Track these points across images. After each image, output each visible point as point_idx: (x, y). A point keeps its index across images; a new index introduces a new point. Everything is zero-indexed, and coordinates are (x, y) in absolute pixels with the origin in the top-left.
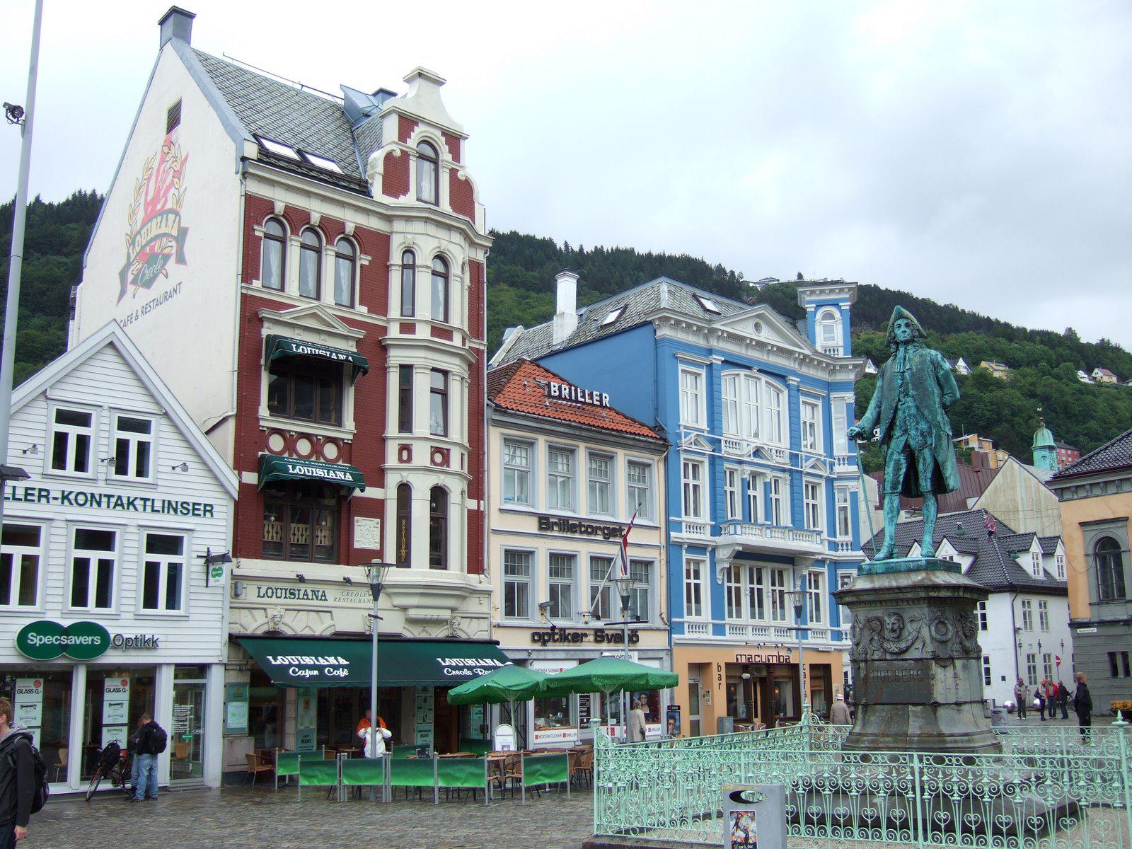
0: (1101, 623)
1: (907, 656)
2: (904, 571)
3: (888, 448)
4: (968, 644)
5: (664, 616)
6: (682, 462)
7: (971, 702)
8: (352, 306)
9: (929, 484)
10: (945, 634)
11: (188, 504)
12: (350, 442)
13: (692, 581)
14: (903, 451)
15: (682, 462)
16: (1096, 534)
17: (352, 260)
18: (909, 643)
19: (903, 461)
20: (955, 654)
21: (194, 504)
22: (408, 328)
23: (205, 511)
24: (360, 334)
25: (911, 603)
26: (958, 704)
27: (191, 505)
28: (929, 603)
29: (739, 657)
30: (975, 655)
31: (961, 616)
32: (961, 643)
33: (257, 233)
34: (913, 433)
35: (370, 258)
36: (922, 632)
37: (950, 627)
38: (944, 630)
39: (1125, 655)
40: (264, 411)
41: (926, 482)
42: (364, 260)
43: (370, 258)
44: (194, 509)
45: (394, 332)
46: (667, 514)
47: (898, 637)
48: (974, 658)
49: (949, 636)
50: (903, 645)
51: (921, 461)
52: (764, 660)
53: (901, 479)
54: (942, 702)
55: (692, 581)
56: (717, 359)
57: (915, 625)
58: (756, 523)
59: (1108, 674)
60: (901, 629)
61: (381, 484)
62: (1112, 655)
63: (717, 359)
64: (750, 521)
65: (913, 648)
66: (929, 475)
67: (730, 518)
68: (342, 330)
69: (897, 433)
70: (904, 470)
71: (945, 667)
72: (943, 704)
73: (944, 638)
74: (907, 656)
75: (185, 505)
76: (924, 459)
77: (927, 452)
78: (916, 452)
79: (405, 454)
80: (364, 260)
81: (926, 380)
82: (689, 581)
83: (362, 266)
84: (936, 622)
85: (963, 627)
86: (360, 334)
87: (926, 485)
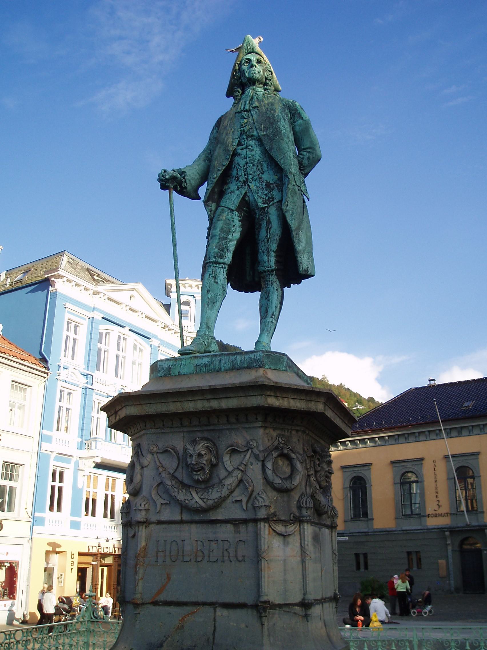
0: (351, 534)
1: (220, 515)
2: (226, 371)
3: (218, 206)
4: (322, 499)
5: (29, 510)
6: (59, 389)
7: (322, 601)
9: (273, 259)
10: (291, 477)
13: (57, 484)
14: (239, 209)
15: (59, 389)
16: (351, 474)
18: (225, 492)
19: (238, 223)
20: (305, 512)
25: (233, 420)
26: (306, 605)
28: (265, 421)
29: (90, 548)
30: (328, 523)
31: (314, 451)
32: (312, 496)
34: (253, 185)
36: (249, 473)
37: (299, 466)
38: (287, 470)
39: (365, 555)
41: (269, 255)
46: (42, 428)
47: (206, 481)
48: (327, 526)
49: (297, 481)
50: (214, 495)
51: (264, 224)
52: (111, 551)
53: (232, 246)
54: (278, 601)
55: (57, 484)
56: (98, 316)
57: (237, 459)
58: (115, 442)
59: (355, 568)
60: (213, 466)
62: (357, 555)
63: (98, 316)
64: (111, 440)
65: (229, 501)
66: (274, 247)
67: (94, 436)
69: (233, 186)
70: (237, 235)
71: (284, 536)
72: (280, 606)
73: (287, 485)
74: (220, 515)
76: (269, 222)
77: (273, 211)
78: (258, 212)
81: (279, 120)
82: (53, 483)
84: (275, 454)
85: (316, 472)
87: (269, 261)
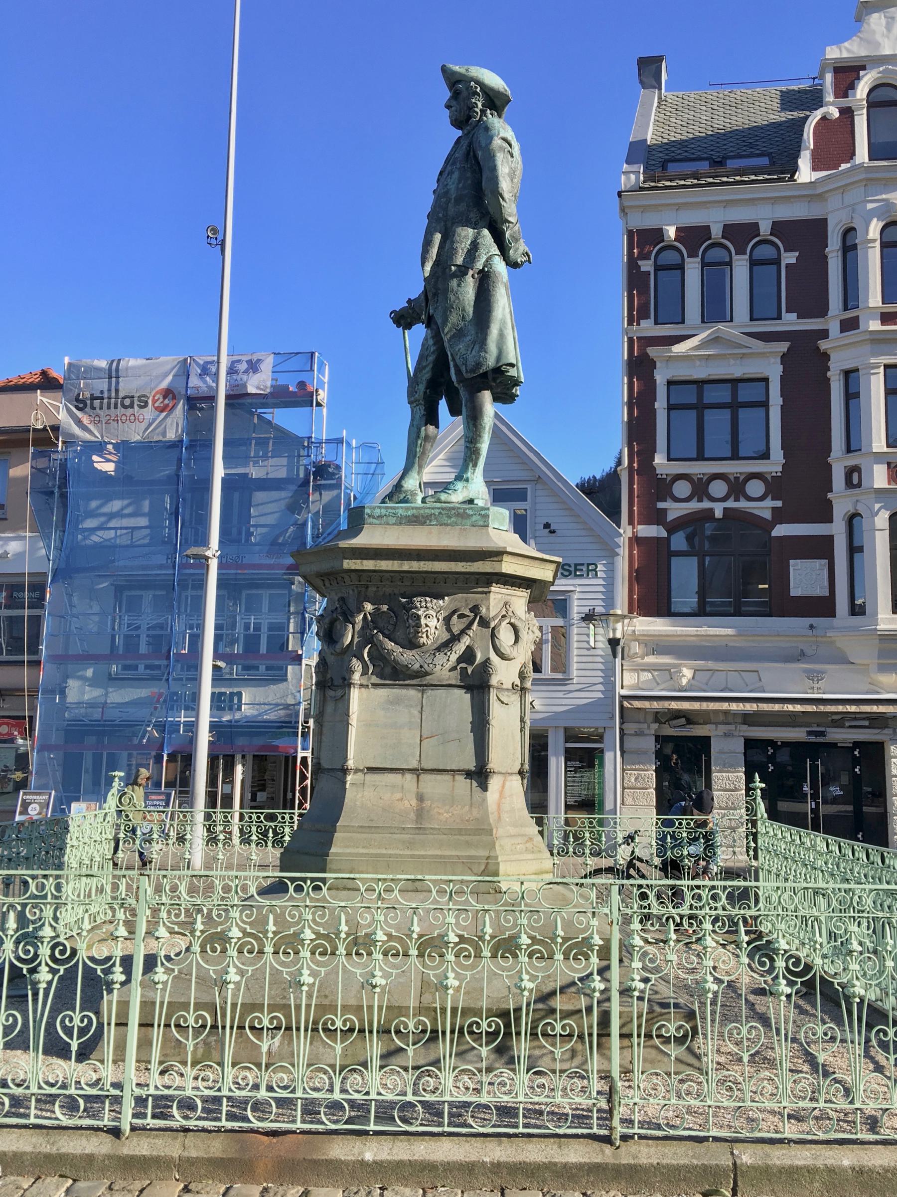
8: (779, 317)
11: (569, 566)
12: (779, 474)
17: (777, 262)
21: (576, 565)
22: (850, 325)
23: (588, 571)
24: (783, 347)
27: (573, 566)
33: (643, 269)
35: (797, 254)
40: (659, 459)
42: (789, 258)
43: (797, 254)
44: (576, 570)
45: (834, 327)
61: (829, 520)
68: (758, 345)
75: (566, 567)
79: (855, 476)
80: (789, 258)
83: (787, 266)
86: (783, 347)
